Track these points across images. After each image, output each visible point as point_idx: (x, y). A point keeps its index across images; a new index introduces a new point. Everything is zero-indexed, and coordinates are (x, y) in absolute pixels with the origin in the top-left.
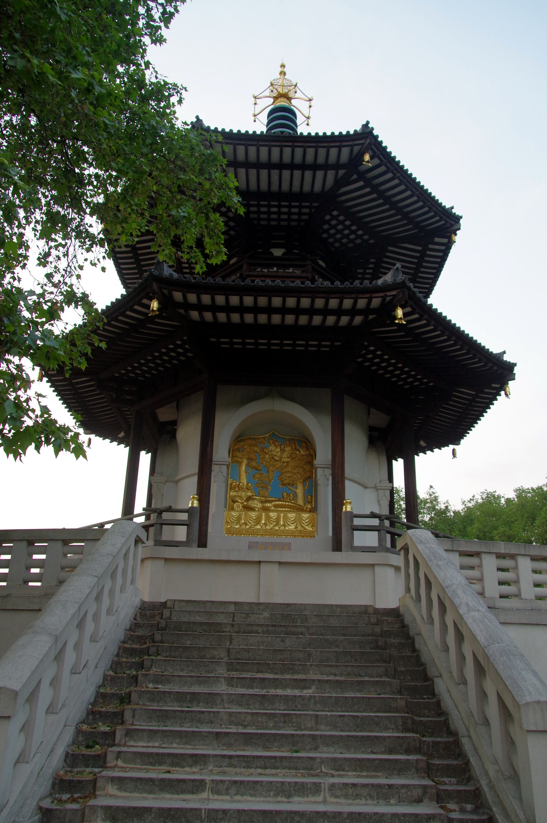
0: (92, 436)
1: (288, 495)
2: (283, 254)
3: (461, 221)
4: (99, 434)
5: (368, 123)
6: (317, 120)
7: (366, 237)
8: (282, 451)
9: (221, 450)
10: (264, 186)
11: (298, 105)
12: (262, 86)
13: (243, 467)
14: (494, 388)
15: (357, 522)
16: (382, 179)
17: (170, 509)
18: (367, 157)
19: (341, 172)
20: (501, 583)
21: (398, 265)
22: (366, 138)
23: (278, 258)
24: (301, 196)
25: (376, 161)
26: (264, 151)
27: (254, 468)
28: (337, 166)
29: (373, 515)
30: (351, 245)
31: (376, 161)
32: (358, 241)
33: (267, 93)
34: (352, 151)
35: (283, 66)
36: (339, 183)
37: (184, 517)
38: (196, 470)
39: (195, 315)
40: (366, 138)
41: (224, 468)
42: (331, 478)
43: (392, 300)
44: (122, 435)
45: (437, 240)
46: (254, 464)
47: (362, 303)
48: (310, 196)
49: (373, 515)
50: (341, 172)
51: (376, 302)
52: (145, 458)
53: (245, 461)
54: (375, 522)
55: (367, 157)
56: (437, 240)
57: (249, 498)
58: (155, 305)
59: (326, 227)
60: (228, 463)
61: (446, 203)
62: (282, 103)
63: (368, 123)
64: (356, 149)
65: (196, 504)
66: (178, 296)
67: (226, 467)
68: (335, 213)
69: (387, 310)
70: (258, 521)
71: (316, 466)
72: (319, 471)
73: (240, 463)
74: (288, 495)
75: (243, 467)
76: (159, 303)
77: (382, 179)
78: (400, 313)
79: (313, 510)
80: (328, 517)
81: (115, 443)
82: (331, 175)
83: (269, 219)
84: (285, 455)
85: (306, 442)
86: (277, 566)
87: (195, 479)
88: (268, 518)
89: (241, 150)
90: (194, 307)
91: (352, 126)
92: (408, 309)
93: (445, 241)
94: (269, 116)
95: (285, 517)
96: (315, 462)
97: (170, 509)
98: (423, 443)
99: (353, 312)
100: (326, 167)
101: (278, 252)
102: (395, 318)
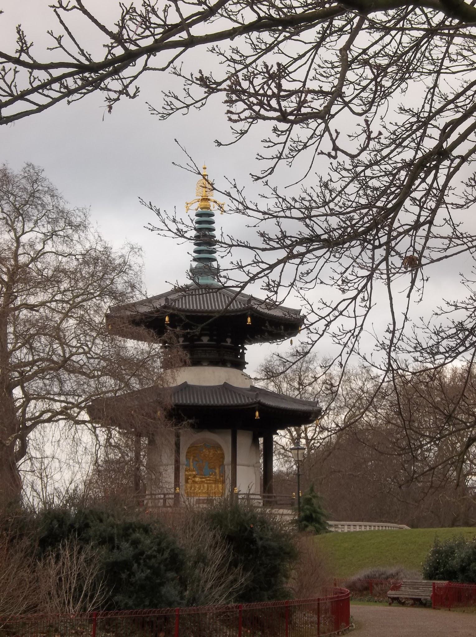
1: (212, 473)
2: (208, 341)
8: (210, 452)
9: (183, 458)
13: (191, 460)
27: (196, 461)
46: (196, 459)
53: (192, 457)
57: (195, 477)
70: (200, 488)
72: (226, 467)
73: (189, 459)
74: (212, 473)
75: (191, 460)
79: (223, 482)
84: (211, 454)
85: (219, 447)
88: (204, 487)
95: (211, 487)
96: (225, 463)
102: (255, 416)
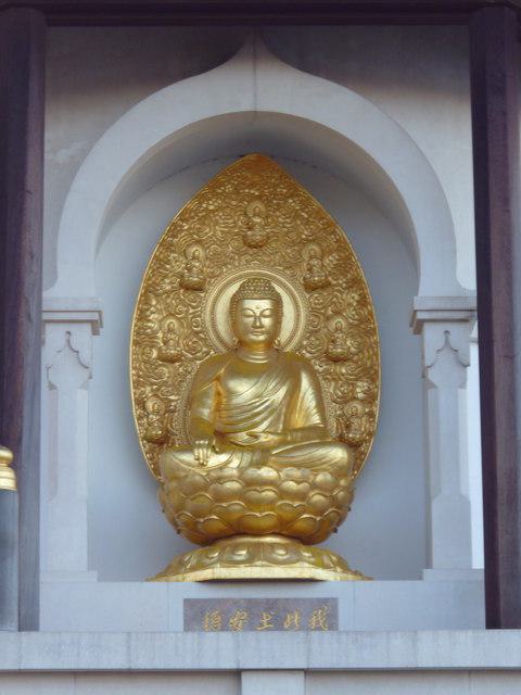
41: (82, 335)
42: (474, 353)
60: (95, 317)
67: (87, 328)
71: (420, 316)
80: (465, 503)
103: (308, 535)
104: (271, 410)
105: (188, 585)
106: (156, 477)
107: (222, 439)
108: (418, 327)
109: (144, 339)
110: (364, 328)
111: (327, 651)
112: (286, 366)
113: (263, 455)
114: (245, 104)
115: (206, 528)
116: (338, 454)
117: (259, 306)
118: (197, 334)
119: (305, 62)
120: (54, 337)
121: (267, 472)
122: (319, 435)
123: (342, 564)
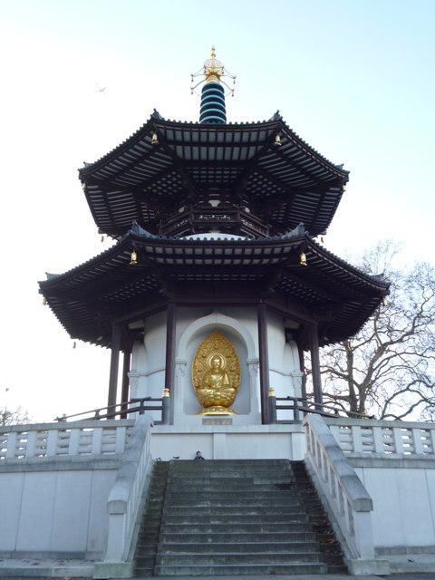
0: (77, 340)
3: (349, 175)
4: (81, 338)
5: (278, 111)
6: (239, 111)
7: (279, 189)
9: (184, 352)
10: (204, 156)
11: (225, 82)
12: (198, 67)
14: (375, 301)
15: (279, 403)
16: (290, 151)
17: (149, 399)
18: (278, 139)
19: (260, 147)
20: (364, 444)
21: (302, 223)
22: (277, 125)
23: (214, 209)
24: (231, 163)
25: (285, 139)
26: (204, 136)
28: (256, 144)
29: (288, 399)
30: (268, 194)
31: (285, 139)
32: (274, 192)
33: (202, 72)
34: (267, 134)
35: (214, 49)
36: (257, 154)
37: (159, 404)
38: (163, 365)
39: (161, 260)
40: (277, 125)
43: (298, 248)
44: (100, 338)
45: (332, 189)
47: (277, 250)
48: (239, 162)
49: (288, 399)
50: (260, 147)
51: (287, 250)
52: (121, 355)
54: (291, 403)
55: (278, 139)
56: (332, 189)
58: (134, 256)
59: (250, 183)
61: (336, 162)
62: (214, 80)
63: (278, 111)
64: (270, 132)
65: (167, 395)
66: (149, 249)
68: (256, 174)
69: (295, 254)
76: (137, 256)
77: (290, 151)
78: (303, 258)
81: (94, 345)
82: (252, 150)
83: (207, 179)
86: (224, 436)
87: (164, 373)
89: (187, 135)
90: (160, 255)
91: (266, 116)
92: (310, 253)
93: (337, 189)
94: (204, 89)
97: (149, 399)
98: (326, 339)
99: (271, 256)
100: (249, 144)
101: (215, 203)
102: (300, 260)
103: (227, 406)
104: (219, 381)
105: (203, 415)
106: (197, 394)
107: (210, 387)
108: (248, 365)
109: (195, 367)
110: (237, 365)
111: (231, 429)
112: (222, 372)
113: (218, 390)
114: (214, 322)
115: (207, 404)
116: (232, 390)
117: (217, 361)
118: (205, 366)
119: (227, 314)
120: (178, 367)
121: (219, 393)
122: (229, 386)
123: (233, 411)
